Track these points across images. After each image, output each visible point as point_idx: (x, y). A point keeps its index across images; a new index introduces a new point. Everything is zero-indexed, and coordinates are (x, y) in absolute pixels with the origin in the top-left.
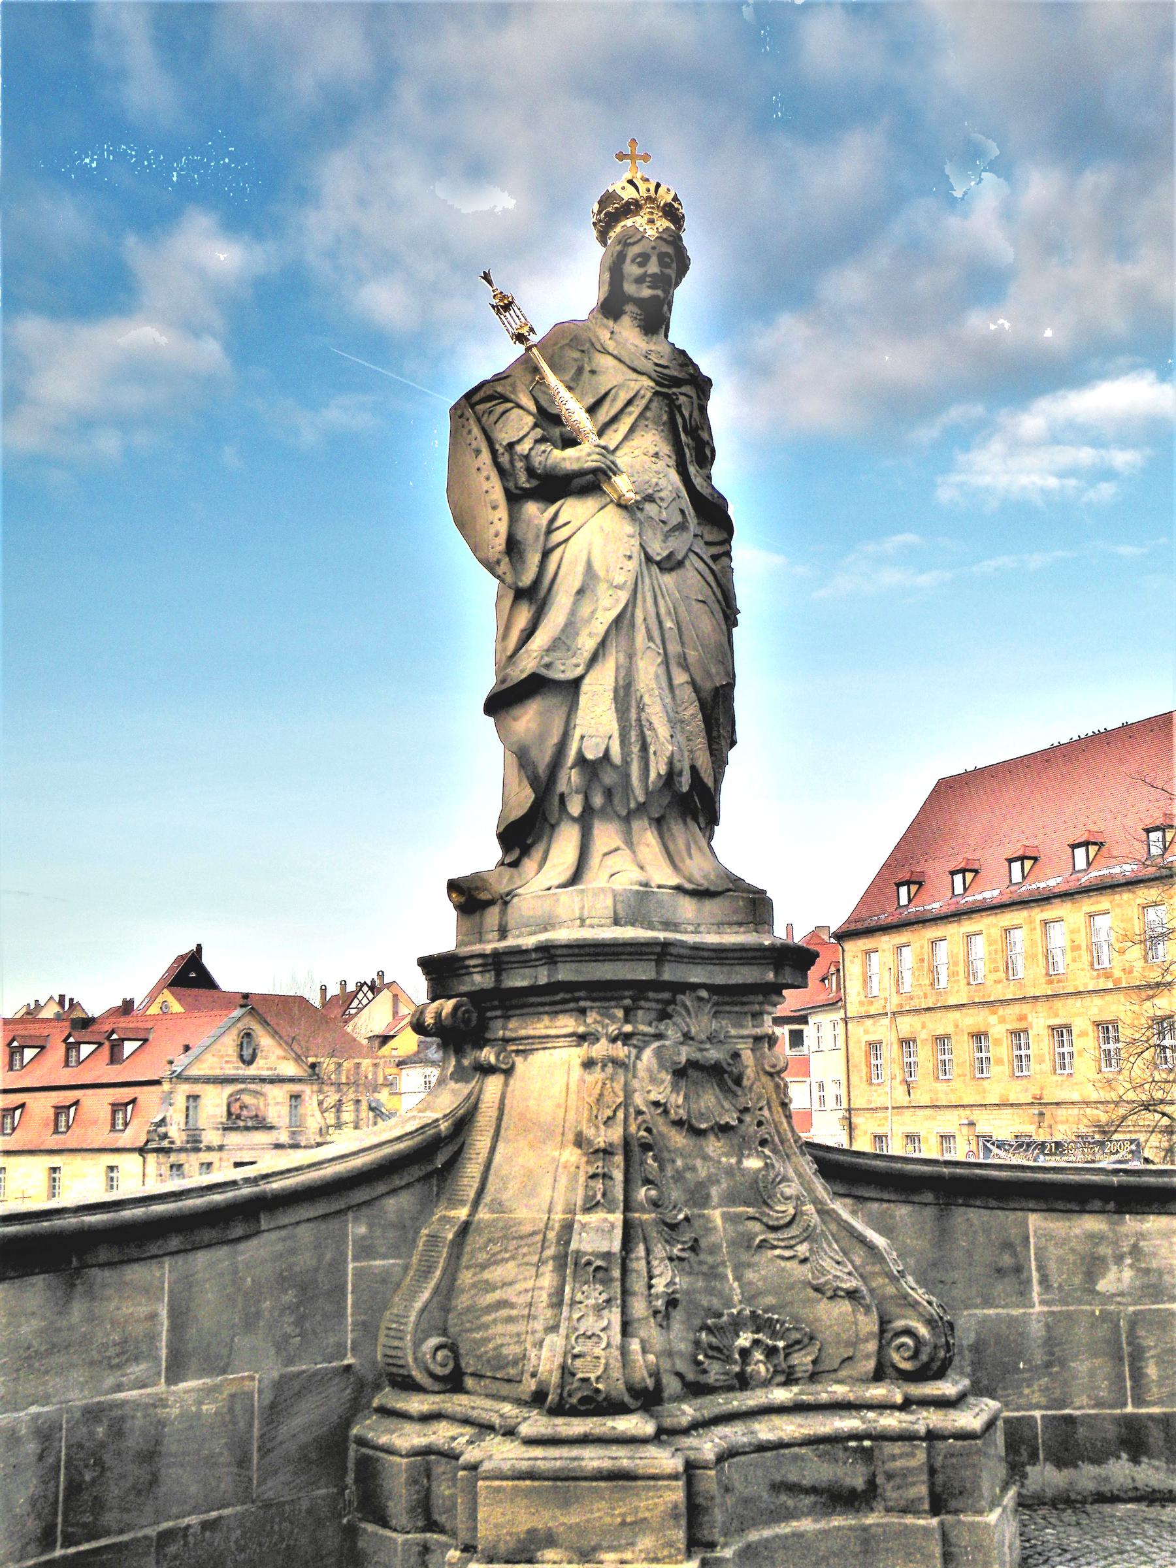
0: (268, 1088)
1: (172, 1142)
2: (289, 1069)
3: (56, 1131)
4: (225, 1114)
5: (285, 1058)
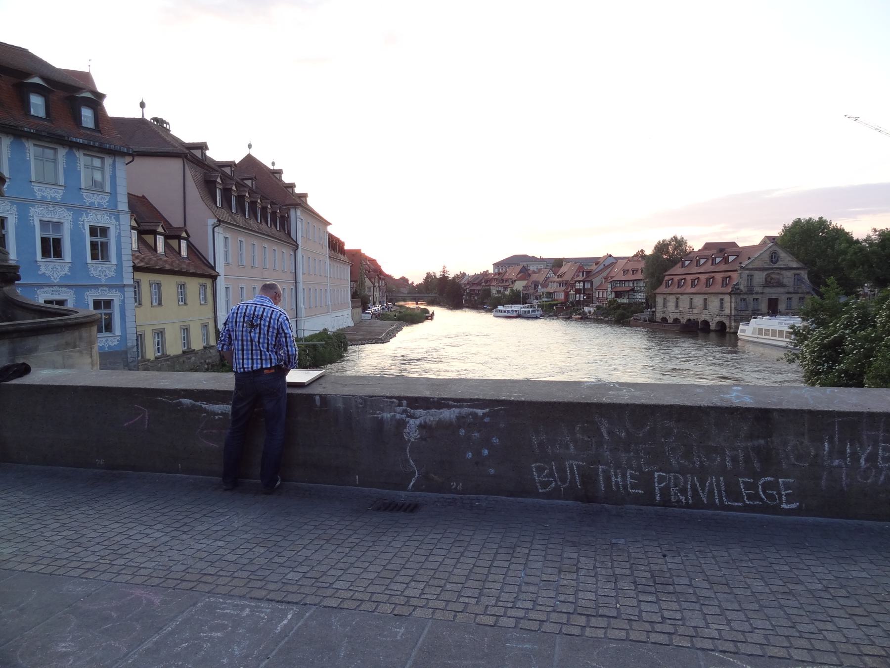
0: (783, 272)
1: (742, 291)
2: (794, 265)
3: (706, 287)
4: (764, 281)
5: (792, 261)
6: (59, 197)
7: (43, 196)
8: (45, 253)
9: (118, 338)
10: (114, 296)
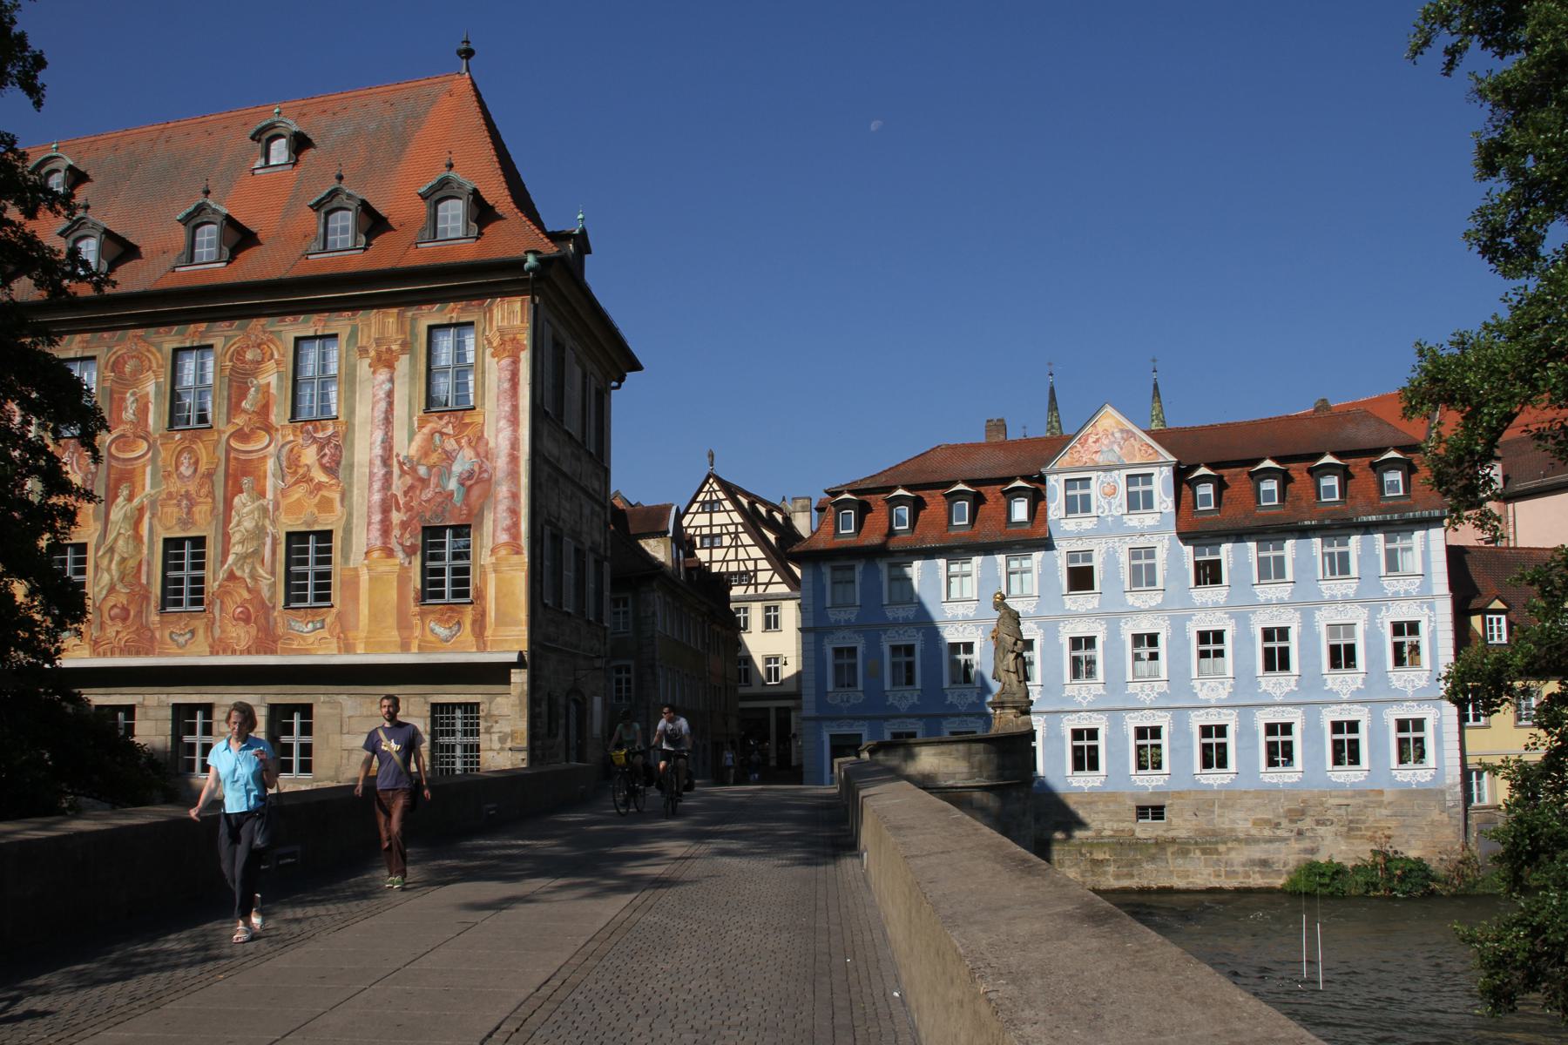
6: (1351, 593)
7: (1332, 596)
8: (1335, 663)
9: (1432, 772)
10: (1429, 714)
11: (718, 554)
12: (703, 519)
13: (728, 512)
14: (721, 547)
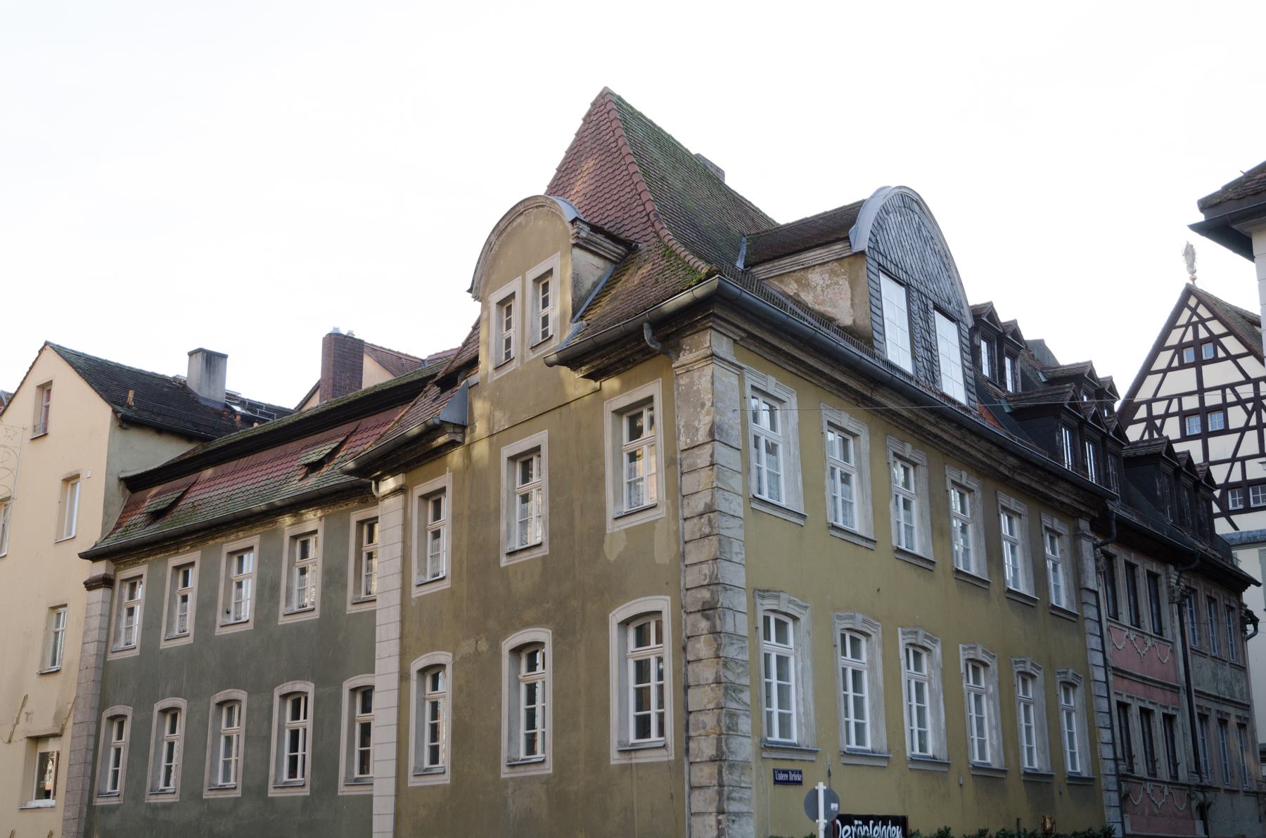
11: (1221, 447)
12: (1183, 380)
13: (1234, 358)
14: (1226, 431)
